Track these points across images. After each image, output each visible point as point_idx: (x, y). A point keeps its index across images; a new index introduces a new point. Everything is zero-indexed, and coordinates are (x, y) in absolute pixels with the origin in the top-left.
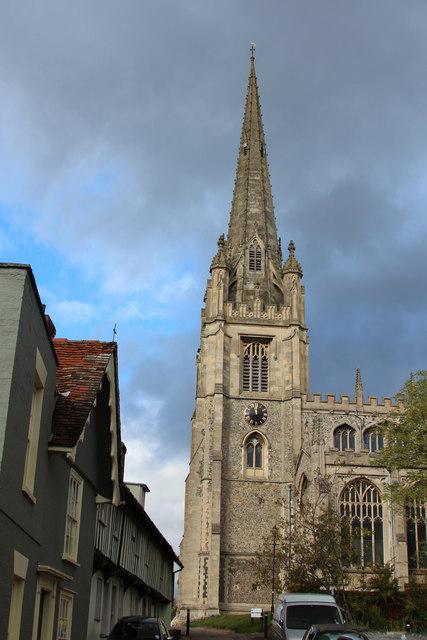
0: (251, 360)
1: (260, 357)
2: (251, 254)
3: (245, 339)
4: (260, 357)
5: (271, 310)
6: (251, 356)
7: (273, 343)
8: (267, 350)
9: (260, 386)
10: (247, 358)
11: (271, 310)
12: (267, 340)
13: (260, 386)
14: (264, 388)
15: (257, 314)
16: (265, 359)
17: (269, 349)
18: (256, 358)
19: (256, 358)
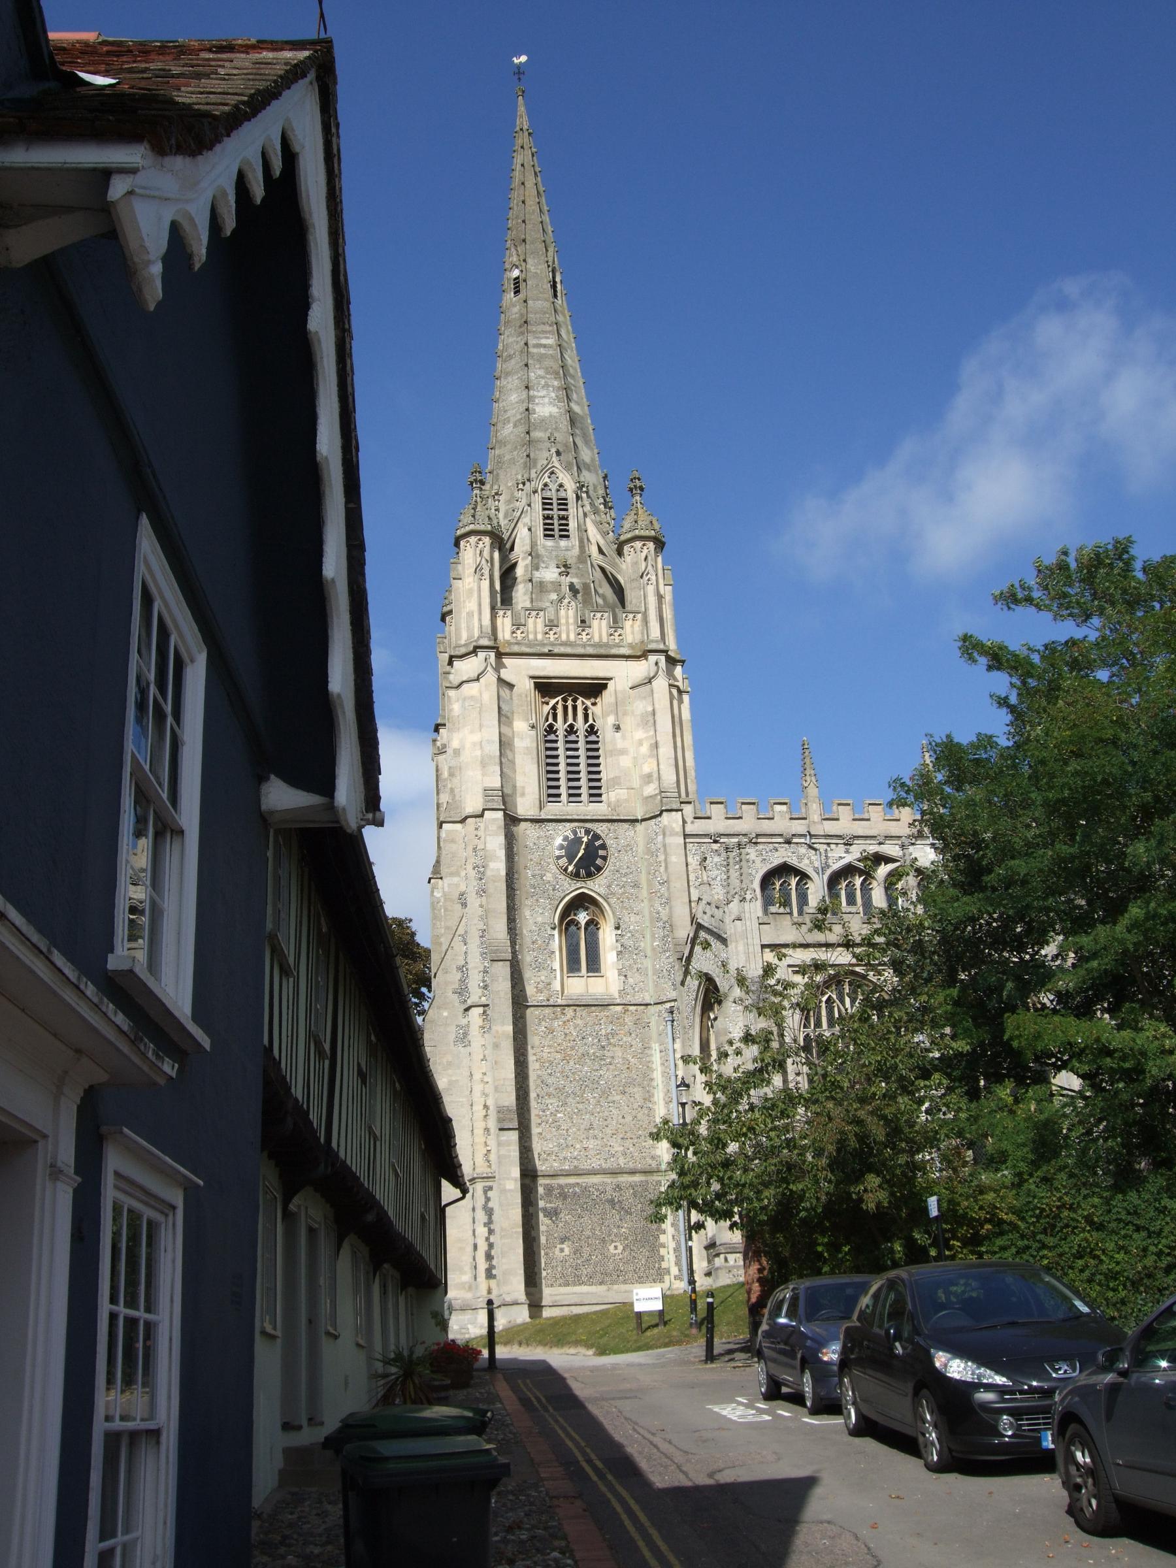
0: (561, 733)
1: (580, 725)
2: (546, 504)
3: (546, 688)
4: (580, 725)
5: (600, 628)
6: (560, 726)
7: (607, 696)
8: (596, 710)
9: (584, 791)
10: (551, 730)
11: (600, 628)
12: (595, 689)
13: (584, 791)
14: (596, 796)
15: (568, 630)
16: (592, 730)
17: (602, 710)
18: (571, 730)
19: (571, 730)
